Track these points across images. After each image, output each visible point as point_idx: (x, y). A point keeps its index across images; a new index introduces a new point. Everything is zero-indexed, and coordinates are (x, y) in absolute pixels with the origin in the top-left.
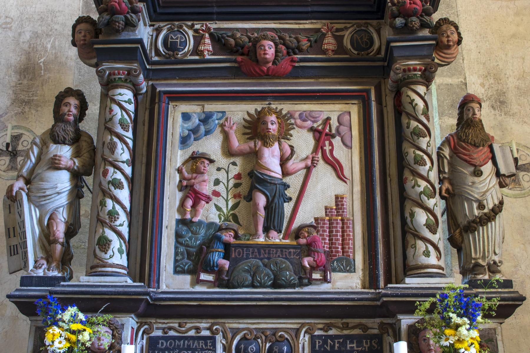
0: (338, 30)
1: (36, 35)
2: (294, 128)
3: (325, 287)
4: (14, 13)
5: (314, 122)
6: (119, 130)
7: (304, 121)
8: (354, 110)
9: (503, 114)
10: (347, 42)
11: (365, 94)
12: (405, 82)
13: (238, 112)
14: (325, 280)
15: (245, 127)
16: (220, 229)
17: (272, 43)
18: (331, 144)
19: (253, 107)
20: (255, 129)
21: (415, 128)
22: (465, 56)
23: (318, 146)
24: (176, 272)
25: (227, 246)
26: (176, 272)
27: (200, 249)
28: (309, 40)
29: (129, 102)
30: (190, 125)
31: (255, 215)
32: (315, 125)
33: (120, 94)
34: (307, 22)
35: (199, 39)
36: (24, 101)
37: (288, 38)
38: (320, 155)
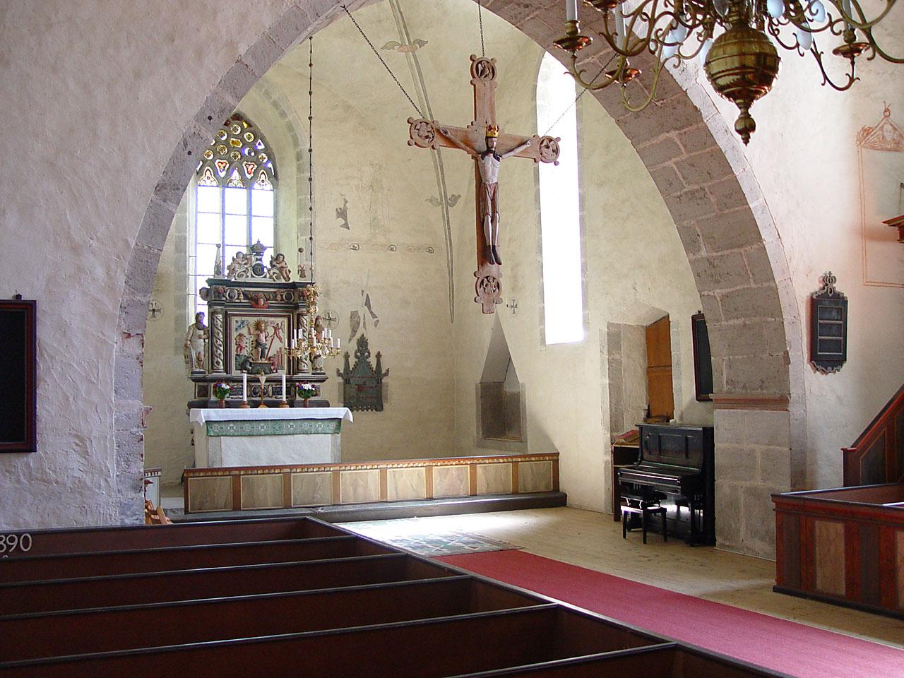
3: (276, 374)
8: (286, 320)
10: (284, 298)
13: (253, 320)
14: (277, 372)
16: (248, 357)
19: (256, 319)
20: (258, 326)
23: (275, 332)
24: (236, 370)
25: (251, 363)
26: (236, 370)
27: (242, 363)
30: (238, 324)
31: (258, 354)
35: (239, 295)
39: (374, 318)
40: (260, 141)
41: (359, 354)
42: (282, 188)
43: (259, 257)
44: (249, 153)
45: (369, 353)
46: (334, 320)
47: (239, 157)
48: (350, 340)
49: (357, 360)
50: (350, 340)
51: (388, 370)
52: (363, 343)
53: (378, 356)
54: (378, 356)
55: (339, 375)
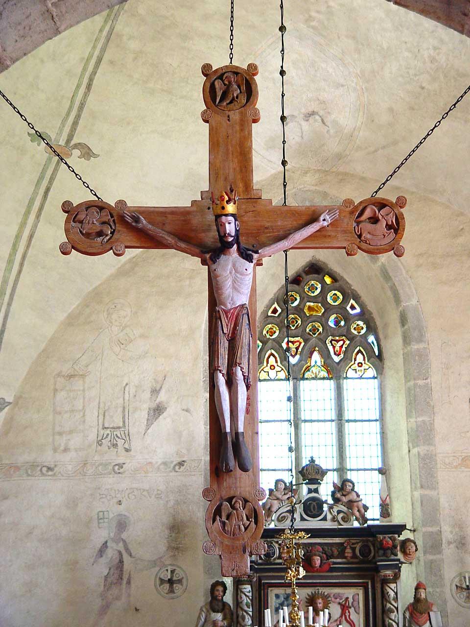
0: (353, 544)
1: (177, 503)
2: (330, 603)
4: (162, 487)
5: (341, 599)
6: (246, 608)
7: (336, 599)
8: (360, 592)
9: (463, 552)
11: (366, 584)
12: (385, 582)
15: (306, 602)
17: (319, 558)
18: (349, 612)
21: (389, 608)
22: (441, 512)
23: (343, 613)
28: (338, 551)
29: (249, 592)
32: (341, 601)
33: (245, 588)
34: (337, 539)
36: (174, 548)
37: (327, 549)
38: (344, 618)
40: (352, 302)
42: (389, 372)
43: (313, 487)
44: (337, 323)
47: (321, 329)
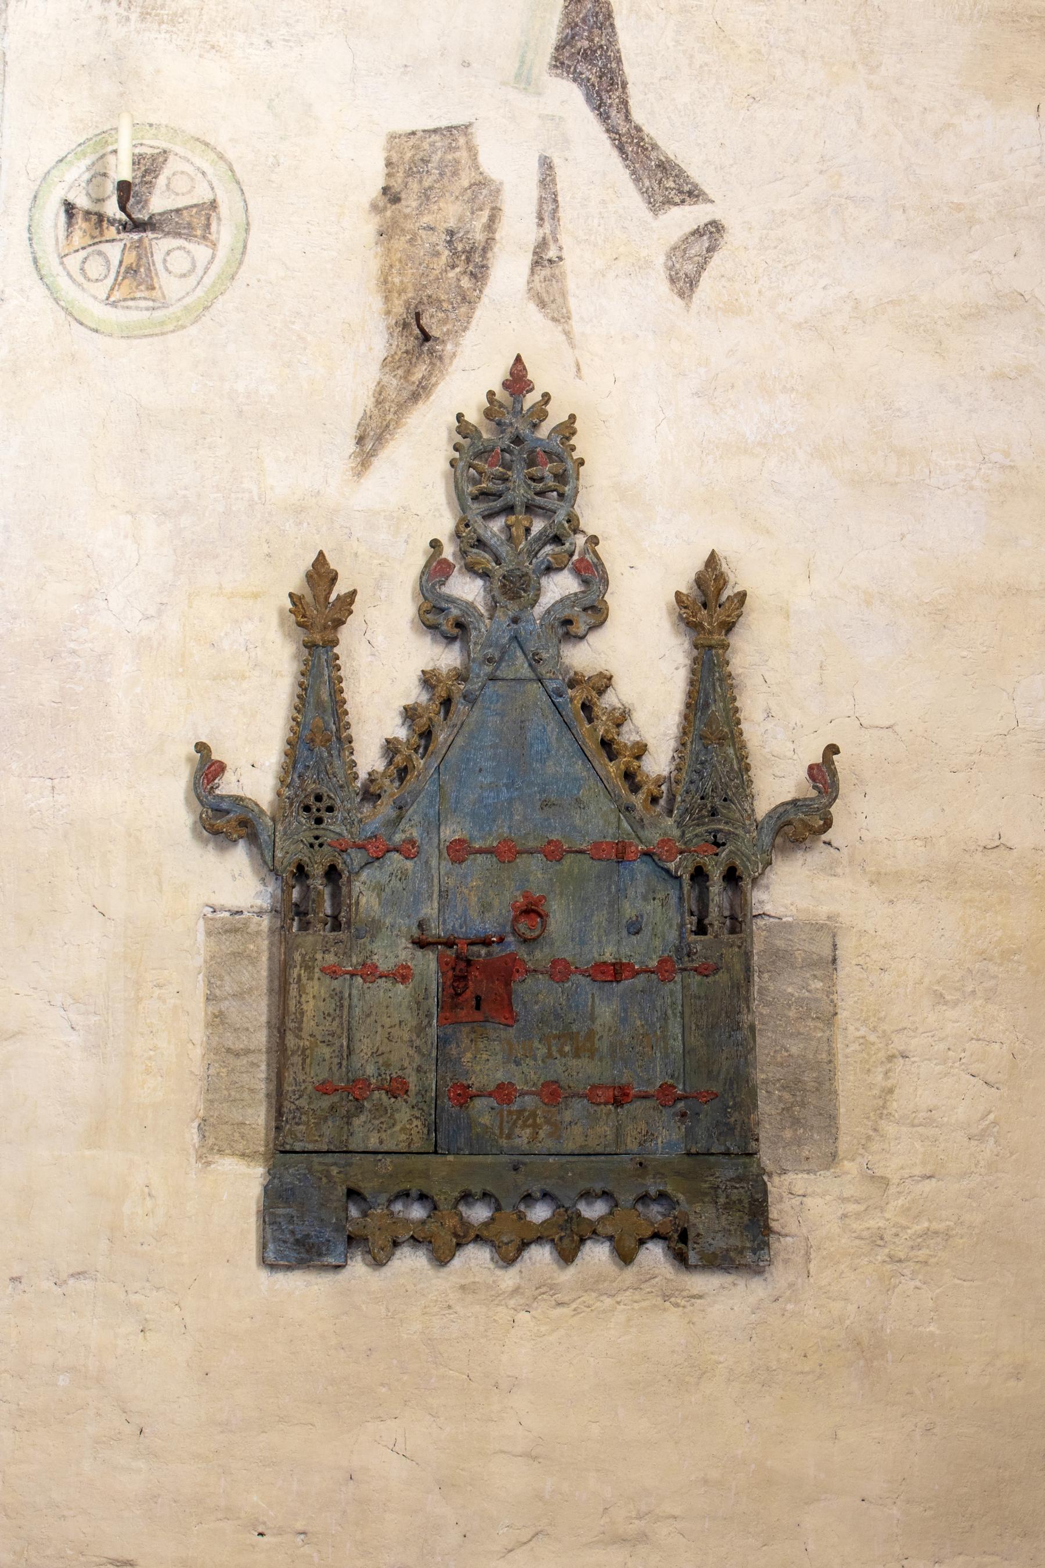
9: (134, 17)
39: (658, 203)
41: (467, 589)
45: (592, 573)
46: (195, 222)
48: (370, 440)
49: (447, 658)
50: (370, 440)
51: (824, 775)
52: (518, 472)
53: (710, 610)
54: (710, 610)
55: (223, 819)
